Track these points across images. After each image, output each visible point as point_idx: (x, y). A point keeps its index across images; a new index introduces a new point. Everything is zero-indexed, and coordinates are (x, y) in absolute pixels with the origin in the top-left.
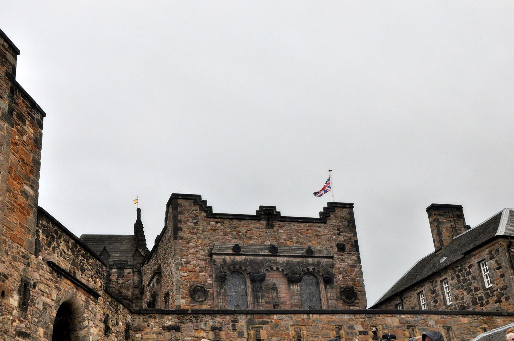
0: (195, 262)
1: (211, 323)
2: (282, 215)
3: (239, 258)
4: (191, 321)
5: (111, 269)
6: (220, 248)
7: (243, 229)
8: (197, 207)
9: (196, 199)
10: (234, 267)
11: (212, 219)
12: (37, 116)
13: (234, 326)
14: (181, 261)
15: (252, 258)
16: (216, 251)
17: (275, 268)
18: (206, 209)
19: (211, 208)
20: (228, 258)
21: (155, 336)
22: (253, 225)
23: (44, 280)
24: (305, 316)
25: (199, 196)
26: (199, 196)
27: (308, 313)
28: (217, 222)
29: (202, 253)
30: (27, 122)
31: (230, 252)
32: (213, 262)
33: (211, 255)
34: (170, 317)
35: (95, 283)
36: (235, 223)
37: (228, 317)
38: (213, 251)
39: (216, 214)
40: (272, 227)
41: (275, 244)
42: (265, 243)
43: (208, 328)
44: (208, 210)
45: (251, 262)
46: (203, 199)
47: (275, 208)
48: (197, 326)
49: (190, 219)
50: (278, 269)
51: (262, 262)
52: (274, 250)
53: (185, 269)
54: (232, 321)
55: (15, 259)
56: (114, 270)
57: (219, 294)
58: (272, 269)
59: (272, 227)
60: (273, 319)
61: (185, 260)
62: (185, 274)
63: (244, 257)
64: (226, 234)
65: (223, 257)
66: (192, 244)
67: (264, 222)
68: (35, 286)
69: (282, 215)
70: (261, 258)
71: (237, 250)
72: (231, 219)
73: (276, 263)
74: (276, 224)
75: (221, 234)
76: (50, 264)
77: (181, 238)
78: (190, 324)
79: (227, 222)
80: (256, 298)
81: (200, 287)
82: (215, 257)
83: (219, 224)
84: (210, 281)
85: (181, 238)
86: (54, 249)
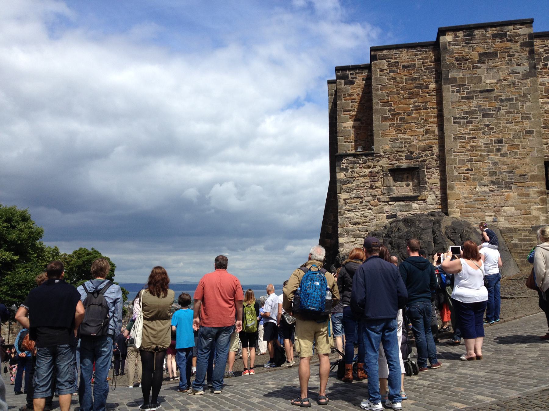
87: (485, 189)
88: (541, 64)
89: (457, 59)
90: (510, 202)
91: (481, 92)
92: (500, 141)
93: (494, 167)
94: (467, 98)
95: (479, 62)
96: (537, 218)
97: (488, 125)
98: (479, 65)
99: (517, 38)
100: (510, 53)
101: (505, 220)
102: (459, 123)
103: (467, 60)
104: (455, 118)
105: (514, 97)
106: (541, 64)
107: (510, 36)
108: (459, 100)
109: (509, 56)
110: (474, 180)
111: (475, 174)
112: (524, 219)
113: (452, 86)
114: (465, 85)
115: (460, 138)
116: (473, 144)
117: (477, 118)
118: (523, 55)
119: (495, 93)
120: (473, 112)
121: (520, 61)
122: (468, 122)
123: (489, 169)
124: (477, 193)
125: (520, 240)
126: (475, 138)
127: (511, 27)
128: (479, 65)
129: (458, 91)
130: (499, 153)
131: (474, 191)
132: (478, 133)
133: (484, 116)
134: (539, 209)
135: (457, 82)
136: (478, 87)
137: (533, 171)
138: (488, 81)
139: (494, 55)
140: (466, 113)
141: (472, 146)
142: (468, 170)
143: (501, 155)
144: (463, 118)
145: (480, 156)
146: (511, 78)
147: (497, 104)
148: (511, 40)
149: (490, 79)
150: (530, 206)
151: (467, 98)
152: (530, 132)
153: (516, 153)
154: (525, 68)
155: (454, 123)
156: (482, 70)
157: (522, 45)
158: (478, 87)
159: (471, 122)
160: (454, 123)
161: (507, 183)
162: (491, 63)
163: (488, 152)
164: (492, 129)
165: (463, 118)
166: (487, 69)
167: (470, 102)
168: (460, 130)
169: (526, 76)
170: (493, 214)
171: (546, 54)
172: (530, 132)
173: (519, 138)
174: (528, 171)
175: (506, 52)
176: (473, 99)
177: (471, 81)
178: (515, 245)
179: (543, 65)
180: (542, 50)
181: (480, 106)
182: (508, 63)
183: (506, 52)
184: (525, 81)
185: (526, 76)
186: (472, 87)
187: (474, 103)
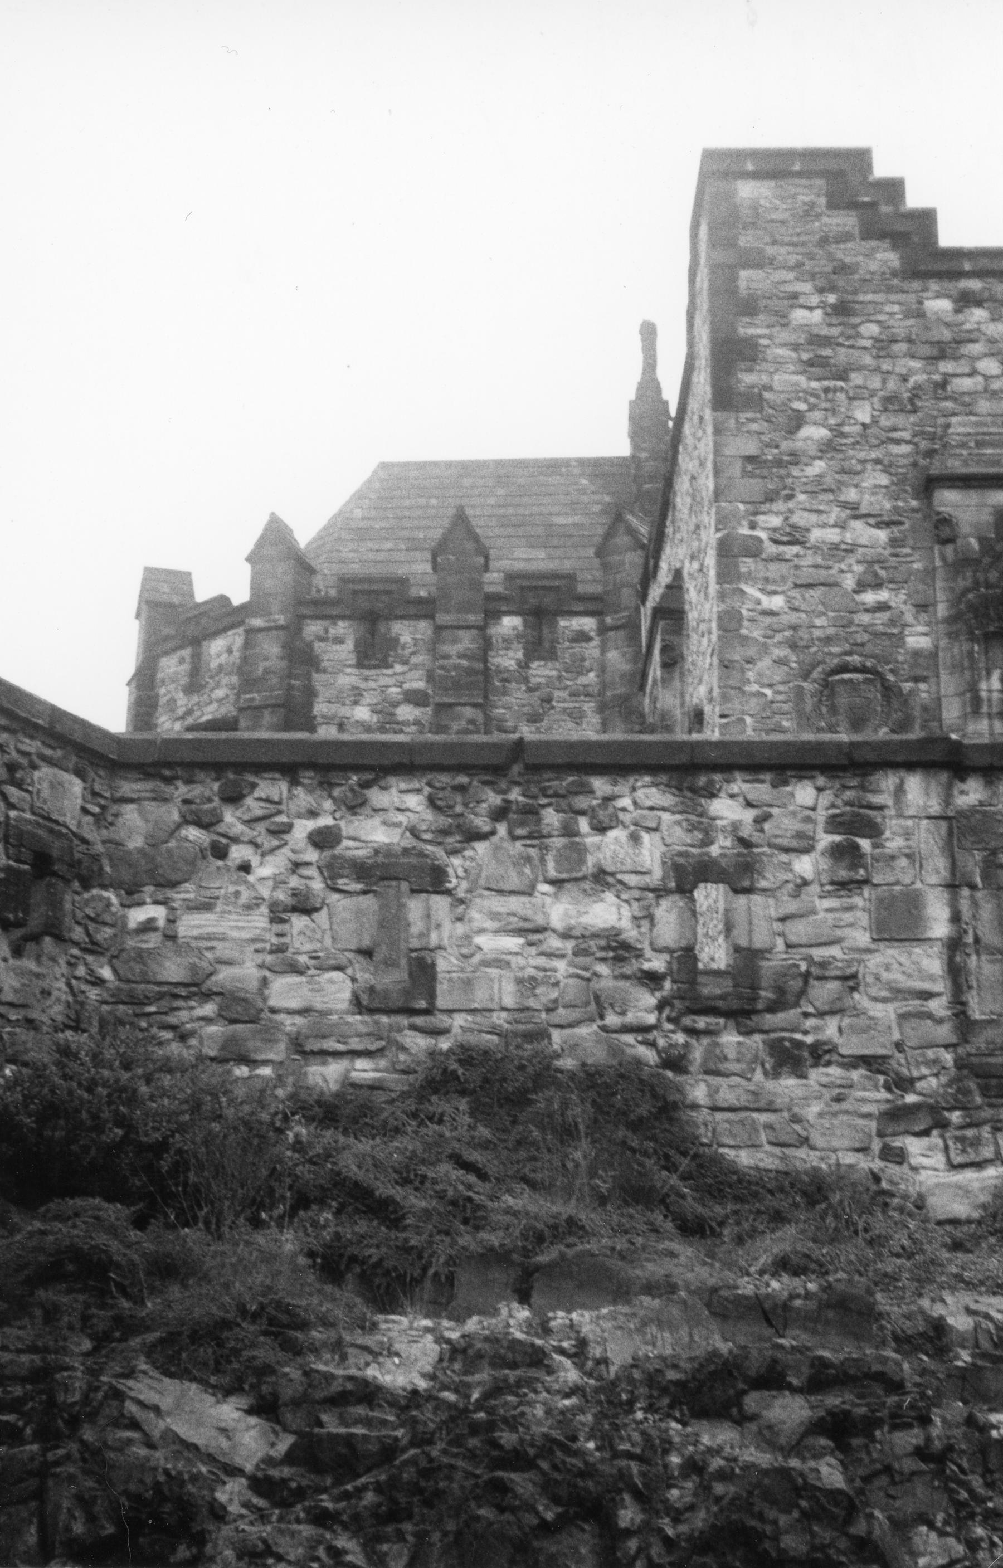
0: (832, 535)
5: (493, 615)
6: (979, 444)
11: (934, 285)
14: (753, 526)
16: (955, 466)
18: (899, 227)
19: (926, 218)
28: (965, 301)
38: (936, 468)
39: (957, 254)
49: (807, 287)
53: (774, 569)
56: (510, 623)
61: (776, 521)
62: (777, 602)
66: (814, 433)
81: (864, 669)
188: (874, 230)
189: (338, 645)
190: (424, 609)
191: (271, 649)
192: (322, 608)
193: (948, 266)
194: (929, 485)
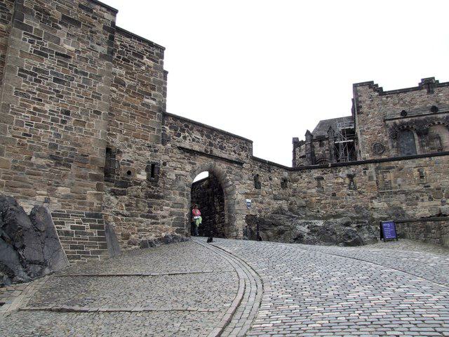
1: (346, 172)
2: (440, 82)
3: (406, 120)
4: (332, 172)
7: (408, 99)
8: (372, 90)
9: (370, 85)
10: (403, 127)
12: (156, 51)
13: (365, 172)
15: (417, 118)
17: (436, 123)
19: (381, 88)
20: (397, 121)
21: (306, 184)
22: (416, 94)
23: (174, 159)
24: (427, 159)
25: (372, 82)
26: (372, 82)
27: (430, 156)
28: (387, 97)
29: (379, 121)
30: (145, 57)
31: (399, 117)
32: (387, 126)
33: (385, 121)
34: (316, 170)
35: (239, 155)
36: (401, 95)
37: (360, 166)
39: (385, 92)
40: (433, 92)
41: (436, 105)
42: (428, 106)
43: (344, 176)
44: (380, 91)
45: (416, 121)
46: (375, 83)
47: (434, 78)
48: (336, 175)
50: (439, 123)
51: (424, 120)
52: (434, 110)
54: (364, 169)
55: (140, 149)
57: (393, 147)
58: (434, 124)
59: (433, 92)
60: (398, 164)
63: (410, 119)
64: (395, 104)
65: (394, 121)
67: (426, 90)
68: (164, 164)
69: (440, 82)
70: (424, 117)
71: (404, 114)
72: (398, 93)
73: (438, 119)
74: (436, 90)
75: (392, 105)
76: (180, 148)
77: (362, 113)
78: (331, 174)
79: (395, 96)
80: (422, 146)
82: (387, 122)
83: (389, 99)
84: (385, 139)
85: (362, 113)
86: (185, 138)
87: (42, 162)
88: (116, 55)
89: (36, 8)
90: (67, 181)
91: (57, 54)
92: (67, 113)
93: (56, 139)
94: (40, 53)
95: (60, 23)
96: (92, 204)
97: (58, 91)
98: (59, 25)
99: (101, 19)
100: (93, 29)
101: (59, 201)
102: (25, 77)
103: (50, 15)
104: (21, 70)
105: (89, 73)
106: (116, 55)
107: (95, 13)
108: (31, 51)
109: (91, 32)
110: (31, 147)
111: (33, 142)
112: (79, 203)
113: (25, 33)
114: (41, 39)
115: (23, 95)
116: (37, 106)
117: (47, 79)
118: (104, 37)
119: (71, 62)
120: (46, 73)
121: (100, 41)
122: (36, 80)
123: (51, 140)
124: (32, 164)
125: (73, 227)
126: (41, 100)
127: (98, 7)
128: (59, 25)
129: (31, 42)
130: (64, 125)
131: (28, 161)
132: (46, 96)
133: (56, 80)
134: (95, 194)
135: (31, 32)
136: (54, 47)
137: (95, 153)
138: (66, 46)
139: (77, 23)
140: (36, 69)
141: (35, 109)
142: (25, 134)
143: (66, 127)
144: (31, 74)
145: (43, 122)
146: (89, 54)
147: (71, 73)
148: (96, 19)
149: (69, 45)
150: (86, 190)
151: (40, 53)
152: (98, 113)
153: (81, 130)
154: (103, 49)
155: (19, 75)
156: (62, 32)
157: (105, 28)
158: (54, 47)
159: (40, 82)
160: (19, 75)
161: (67, 160)
162: (73, 30)
163: (53, 120)
164: (62, 97)
165: (31, 74)
166: (68, 34)
167: (42, 59)
168: (25, 87)
169: (103, 57)
170: (45, 193)
171: (122, 48)
172: (98, 113)
173: (87, 115)
174: (90, 152)
175: (89, 27)
176: (46, 56)
177: (48, 37)
178: (67, 233)
179: (117, 57)
180: (118, 43)
181: (53, 68)
182: (89, 38)
183: (89, 27)
184: (101, 62)
185: (103, 57)
186: (47, 44)
187: (47, 62)
188: (375, 90)
189: (317, 145)
190: (327, 139)
191: (309, 146)
192: (315, 140)
193: (385, 93)
194: (385, 121)
